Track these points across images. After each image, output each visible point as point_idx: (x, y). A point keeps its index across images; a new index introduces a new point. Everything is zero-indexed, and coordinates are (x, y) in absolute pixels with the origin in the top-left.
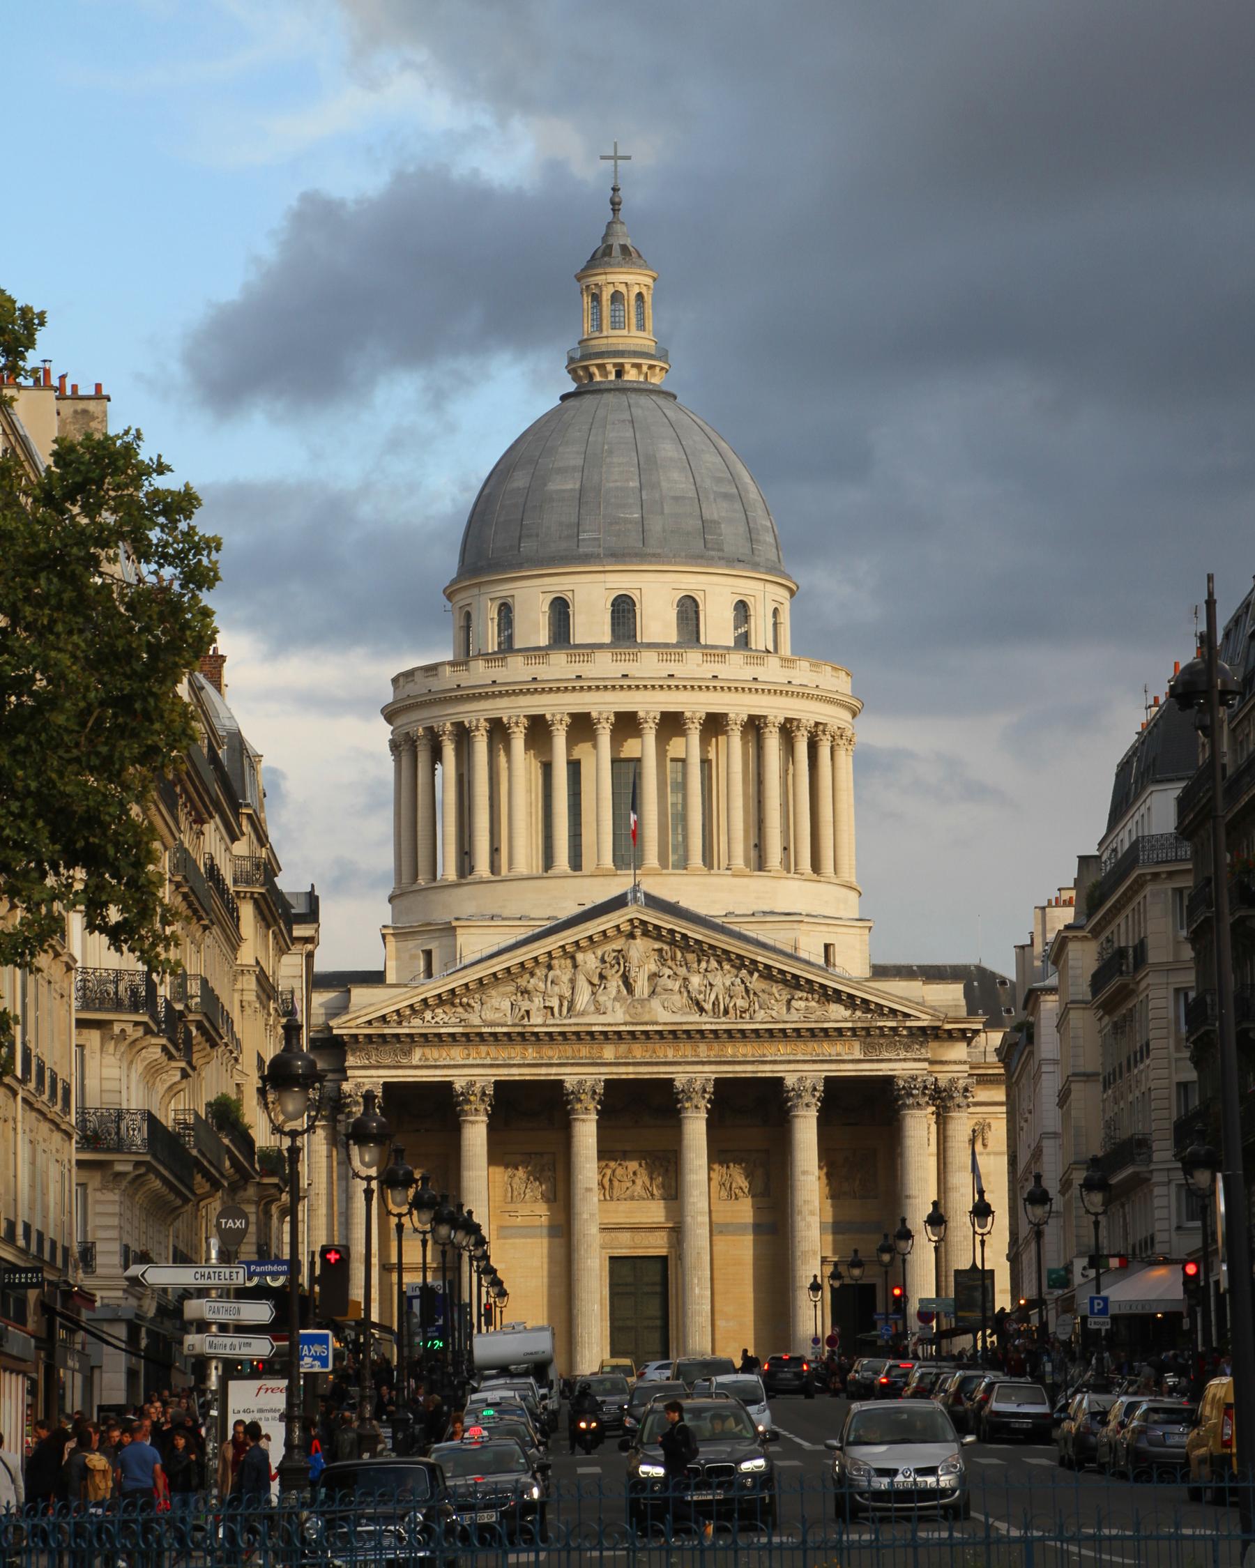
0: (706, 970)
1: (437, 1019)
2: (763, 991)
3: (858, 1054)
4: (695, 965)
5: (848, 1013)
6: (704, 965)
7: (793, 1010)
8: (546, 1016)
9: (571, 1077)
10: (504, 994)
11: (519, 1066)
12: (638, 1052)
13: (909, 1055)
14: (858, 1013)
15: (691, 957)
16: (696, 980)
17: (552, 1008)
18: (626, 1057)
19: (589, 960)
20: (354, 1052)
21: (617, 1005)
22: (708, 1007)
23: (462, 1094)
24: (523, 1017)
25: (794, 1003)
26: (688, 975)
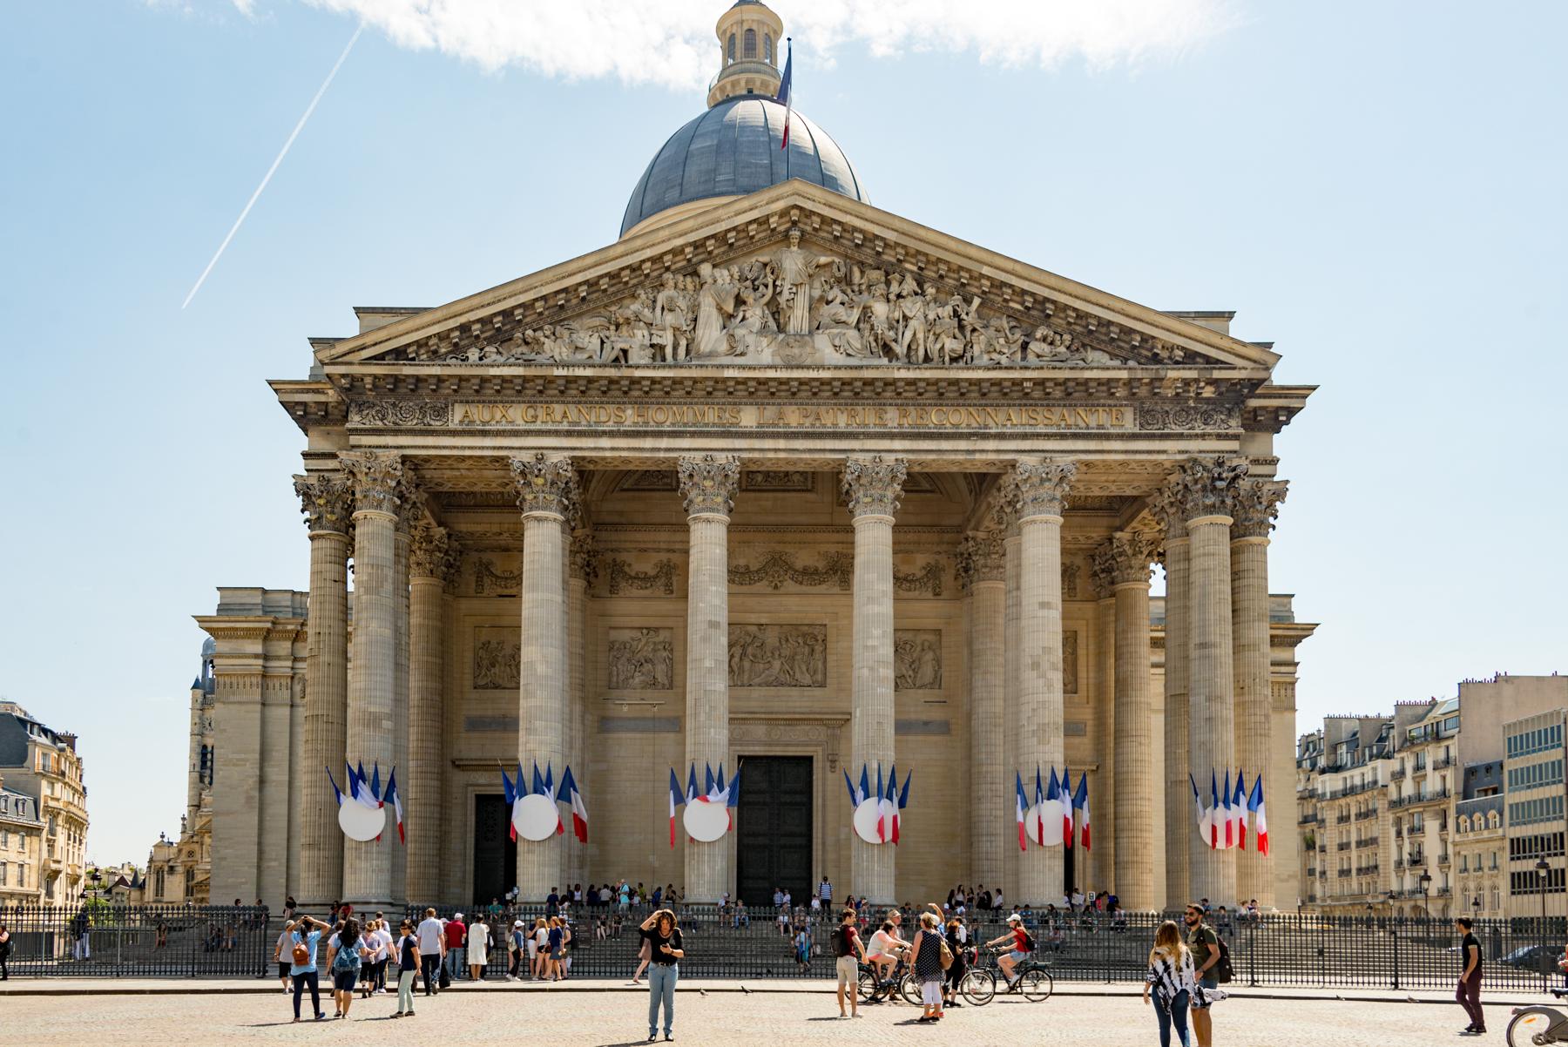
0: (899, 296)
1: (485, 361)
2: (986, 327)
3: (1129, 424)
4: (883, 286)
5: (1117, 363)
6: (895, 288)
7: (1031, 357)
8: (654, 358)
9: (688, 452)
10: (594, 329)
11: (611, 434)
12: (794, 418)
13: (1209, 430)
14: (1131, 363)
15: (876, 275)
16: (880, 309)
17: (662, 348)
18: (776, 425)
19: (723, 278)
20: (361, 407)
21: (765, 341)
22: (900, 349)
23: (522, 473)
24: (617, 359)
25: (1035, 347)
26: (871, 303)
